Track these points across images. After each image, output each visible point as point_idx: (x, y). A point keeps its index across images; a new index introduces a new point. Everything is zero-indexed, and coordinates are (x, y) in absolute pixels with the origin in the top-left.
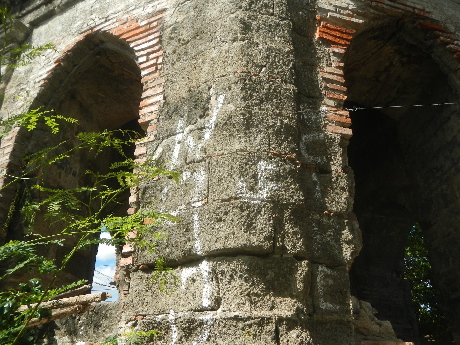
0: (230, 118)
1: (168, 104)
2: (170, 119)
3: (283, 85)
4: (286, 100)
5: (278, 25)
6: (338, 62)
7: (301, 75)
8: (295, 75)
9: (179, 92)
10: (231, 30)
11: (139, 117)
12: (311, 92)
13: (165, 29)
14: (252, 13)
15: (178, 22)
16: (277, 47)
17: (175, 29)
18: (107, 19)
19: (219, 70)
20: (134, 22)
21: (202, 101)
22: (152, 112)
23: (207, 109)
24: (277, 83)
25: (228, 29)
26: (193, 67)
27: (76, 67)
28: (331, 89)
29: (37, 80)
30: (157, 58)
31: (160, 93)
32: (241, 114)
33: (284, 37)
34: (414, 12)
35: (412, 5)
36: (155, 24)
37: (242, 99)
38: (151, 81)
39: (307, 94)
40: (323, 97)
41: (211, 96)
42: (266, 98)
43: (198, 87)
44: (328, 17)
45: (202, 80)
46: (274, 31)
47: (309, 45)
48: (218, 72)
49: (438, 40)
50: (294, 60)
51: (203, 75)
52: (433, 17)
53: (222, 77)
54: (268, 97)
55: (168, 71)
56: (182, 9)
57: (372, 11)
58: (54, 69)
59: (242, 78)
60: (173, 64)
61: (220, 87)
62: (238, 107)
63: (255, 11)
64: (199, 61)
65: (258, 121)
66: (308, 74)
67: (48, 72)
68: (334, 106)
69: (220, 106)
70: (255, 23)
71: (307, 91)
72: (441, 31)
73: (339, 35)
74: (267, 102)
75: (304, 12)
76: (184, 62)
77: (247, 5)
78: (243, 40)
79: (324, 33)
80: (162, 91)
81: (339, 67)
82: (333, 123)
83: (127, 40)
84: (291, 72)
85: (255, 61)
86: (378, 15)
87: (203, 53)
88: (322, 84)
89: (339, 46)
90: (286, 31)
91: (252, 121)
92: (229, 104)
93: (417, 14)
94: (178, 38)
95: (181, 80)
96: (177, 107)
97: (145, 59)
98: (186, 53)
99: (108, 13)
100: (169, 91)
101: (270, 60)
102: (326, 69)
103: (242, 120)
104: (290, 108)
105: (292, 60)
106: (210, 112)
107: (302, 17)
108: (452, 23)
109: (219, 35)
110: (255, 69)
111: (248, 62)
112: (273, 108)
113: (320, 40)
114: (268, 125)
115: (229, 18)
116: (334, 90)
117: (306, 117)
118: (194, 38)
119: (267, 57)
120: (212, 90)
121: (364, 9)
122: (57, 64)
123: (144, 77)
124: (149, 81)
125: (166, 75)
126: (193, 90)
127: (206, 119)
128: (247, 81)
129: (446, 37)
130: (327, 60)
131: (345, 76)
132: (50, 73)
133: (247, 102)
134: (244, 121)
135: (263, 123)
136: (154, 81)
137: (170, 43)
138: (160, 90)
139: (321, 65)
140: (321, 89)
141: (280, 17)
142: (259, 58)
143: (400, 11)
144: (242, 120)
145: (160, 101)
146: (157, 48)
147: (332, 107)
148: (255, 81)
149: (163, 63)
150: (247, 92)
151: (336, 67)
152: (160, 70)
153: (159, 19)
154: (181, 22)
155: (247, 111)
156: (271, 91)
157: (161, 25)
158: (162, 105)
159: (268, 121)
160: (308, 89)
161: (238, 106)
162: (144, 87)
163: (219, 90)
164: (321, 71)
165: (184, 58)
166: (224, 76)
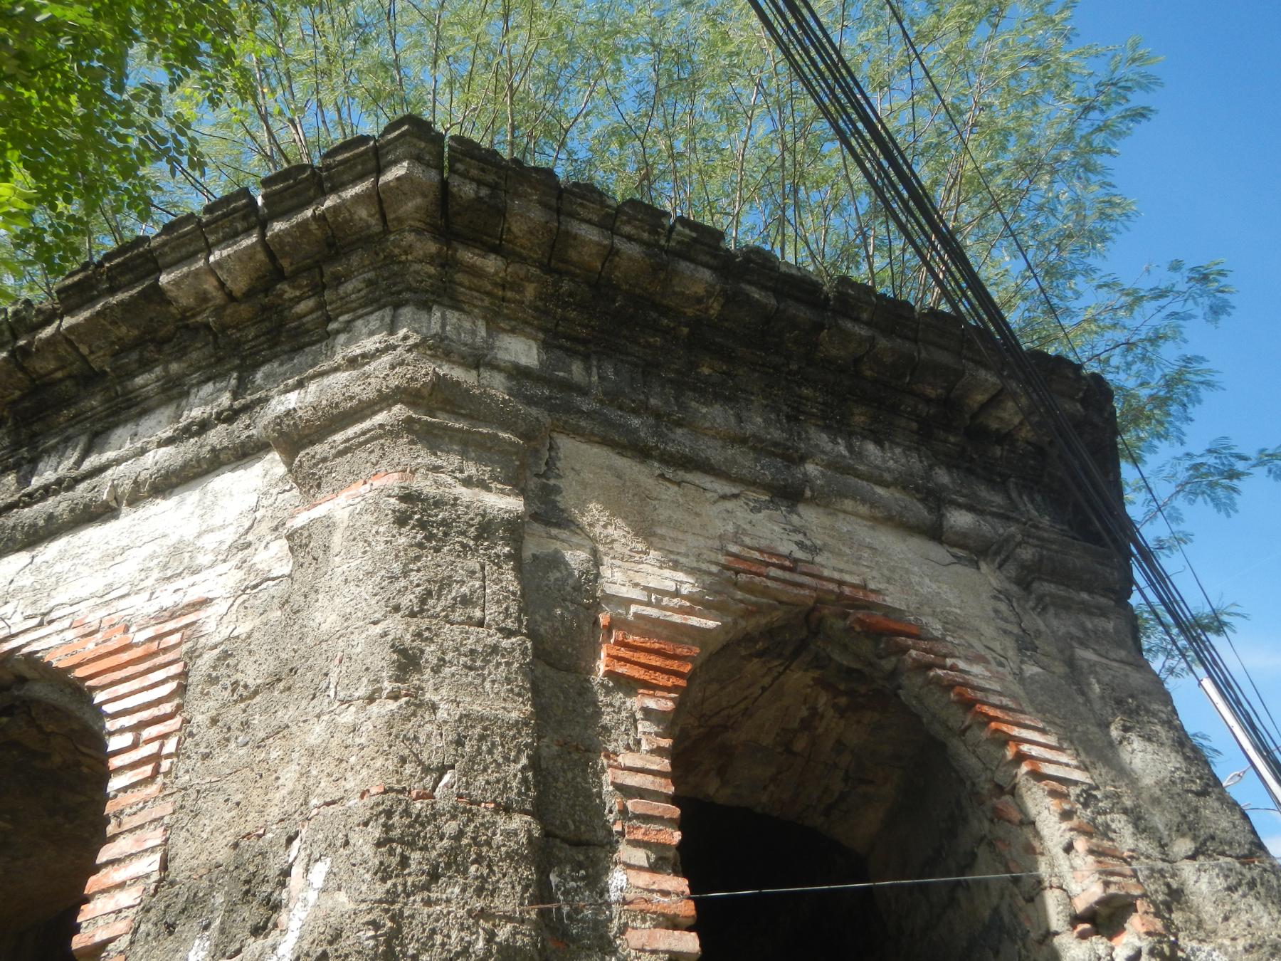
0: (337, 936)
1: (172, 884)
2: (171, 933)
3: (500, 820)
4: (505, 865)
5: (495, 649)
6: (657, 734)
7: (556, 780)
8: (535, 787)
9: (208, 844)
10: (367, 669)
11: (76, 929)
12: (583, 828)
13: (200, 655)
14: (425, 623)
15: (237, 637)
16: (486, 712)
17: (226, 655)
18: (47, 619)
19: (323, 784)
20: (118, 630)
21: (265, 880)
22: (120, 911)
23: (276, 907)
24: (483, 817)
25: (358, 667)
26: (256, 770)
28: (637, 817)
30: (165, 737)
31: (152, 850)
32: (368, 923)
33: (508, 681)
34: (842, 593)
35: (836, 575)
36: (174, 639)
37: (375, 874)
38: (135, 808)
39: (569, 839)
40: (617, 842)
41: (291, 866)
42: (448, 866)
43: (260, 836)
44: (630, 617)
45: (274, 812)
46: (483, 668)
47: (580, 694)
48: (319, 791)
49: (906, 657)
50: (532, 743)
51: (278, 796)
52: (889, 601)
53: (328, 804)
54: (454, 861)
55: (187, 777)
56: (251, 601)
57: (739, 595)
59: (381, 808)
60: (206, 756)
61: (320, 836)
62: (363, 901)
63: (436, 616)
64: (274, 755)
65: (418, 941)
66: (574, 778)
68: (646, 865)
69: (312, 896)
70: (433, 647)
71: (572, 827)
72: (909, 635)
73: (658, 664)
74: (450, 878)
75: (567, 608)
76: (237, 752)
77: (415, 601)
78: (395, 696)
79: (620, 659)
80: (159, 842)
81: (658, 751)
82: (644, 920)
83: (89, 683)
84: (524, 781)
85: (424, 757)
86: (755, 604)
87: (286, 732)
88: (613, 802)
89: (658, 693)
90: (516, 665)
91: (401, 945)
92: (339, 889)
93: (848, 598)
94: (233, 679)
95: (222, 806)
96: (195, 894)
97: (127, 739)
98: (245, 725)
99: (52, 603)
100: (180, 842)
101: (467, 749)
102: (626, 759)
103: (372, 943)
104: (518, 888)
105: (526, 745)
106: (283, 917)
107: (563, 622)
108: (934, 614)
109: (333, 681)
110: (422, 779)
111: (403, 760)
112: (467, 895)
113: (610, 679)
114: (449, 951)
115: (364, 635)
116: (646, 818)
117: (566, 909)
118: (270, 686)
119: (459, 742)
120: (296, 843)
121: (716, 592)
123: (115, 796)
124: (128, 811)
125: (179, 790)
126: (243, 843)
127: (270, 941)
128: (396, 818)
129: (925, 650)
130: (627, 732)
131: (676, 775)
133: (389, 883)
134: (376, 946)
135: (433, 945)
136: (142, 808)
137: (208, 694)
138: (154, 837)
139: (611, 748)
140: (611, 817)
141: (501, 630)
142: (435, 747)
143: (807, 592)
144: (372, 943)
145: (148, 876)
146: (167, 708)
147: (640, 868)
148: (418, 815)
149: (176, 754)
150: (391, 852)
151: (652, 752)
152: (166, 774)
153: (187, 626)
154: (243, 637)
155: (387, 911)
156: (464, 841)
157: (190, 644)
158: (153, 887)
159: (449, 937)
160: (574, 822)
161: (363, 896)
162: (111, 829)
163: (315, 846)
164: (610, 766)
165: (240, 739)
166: (334, 802)
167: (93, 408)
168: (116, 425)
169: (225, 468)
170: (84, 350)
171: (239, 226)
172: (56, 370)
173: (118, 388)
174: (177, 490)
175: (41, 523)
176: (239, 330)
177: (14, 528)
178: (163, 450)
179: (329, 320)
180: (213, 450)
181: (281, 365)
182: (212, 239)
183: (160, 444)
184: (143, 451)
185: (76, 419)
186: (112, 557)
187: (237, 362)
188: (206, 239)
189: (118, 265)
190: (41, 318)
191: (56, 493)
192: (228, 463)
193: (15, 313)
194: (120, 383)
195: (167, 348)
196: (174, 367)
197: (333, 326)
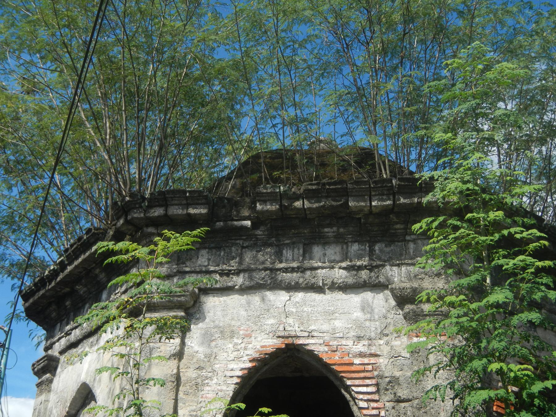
17: (390, 382)
27: (267, 367)
29: (229, 374)
36: (370, 368)
58: (249, 369)
67: (242, 369)
122: (254, 364)
132: (246, 372)
167: (304, 233)
168: (314, 244)
170: (308, 212)
171: (385, 193)
173: (317, 230)
174: (348, 291)
177: (281, 281)
178: (341, 271)
179: (407, 234)
180: (365, 281)
181: (386, 246)
182: (373, 193)
183: (340, 268)
184: (333, 268)
186: (330, 315)
187: (369, 239)
188: (370, 193)
189: (333, 189)
191: (297, 272)
192: (369, 287)
193: (284, 191)
196: (341, 230)
197: (408, 238)
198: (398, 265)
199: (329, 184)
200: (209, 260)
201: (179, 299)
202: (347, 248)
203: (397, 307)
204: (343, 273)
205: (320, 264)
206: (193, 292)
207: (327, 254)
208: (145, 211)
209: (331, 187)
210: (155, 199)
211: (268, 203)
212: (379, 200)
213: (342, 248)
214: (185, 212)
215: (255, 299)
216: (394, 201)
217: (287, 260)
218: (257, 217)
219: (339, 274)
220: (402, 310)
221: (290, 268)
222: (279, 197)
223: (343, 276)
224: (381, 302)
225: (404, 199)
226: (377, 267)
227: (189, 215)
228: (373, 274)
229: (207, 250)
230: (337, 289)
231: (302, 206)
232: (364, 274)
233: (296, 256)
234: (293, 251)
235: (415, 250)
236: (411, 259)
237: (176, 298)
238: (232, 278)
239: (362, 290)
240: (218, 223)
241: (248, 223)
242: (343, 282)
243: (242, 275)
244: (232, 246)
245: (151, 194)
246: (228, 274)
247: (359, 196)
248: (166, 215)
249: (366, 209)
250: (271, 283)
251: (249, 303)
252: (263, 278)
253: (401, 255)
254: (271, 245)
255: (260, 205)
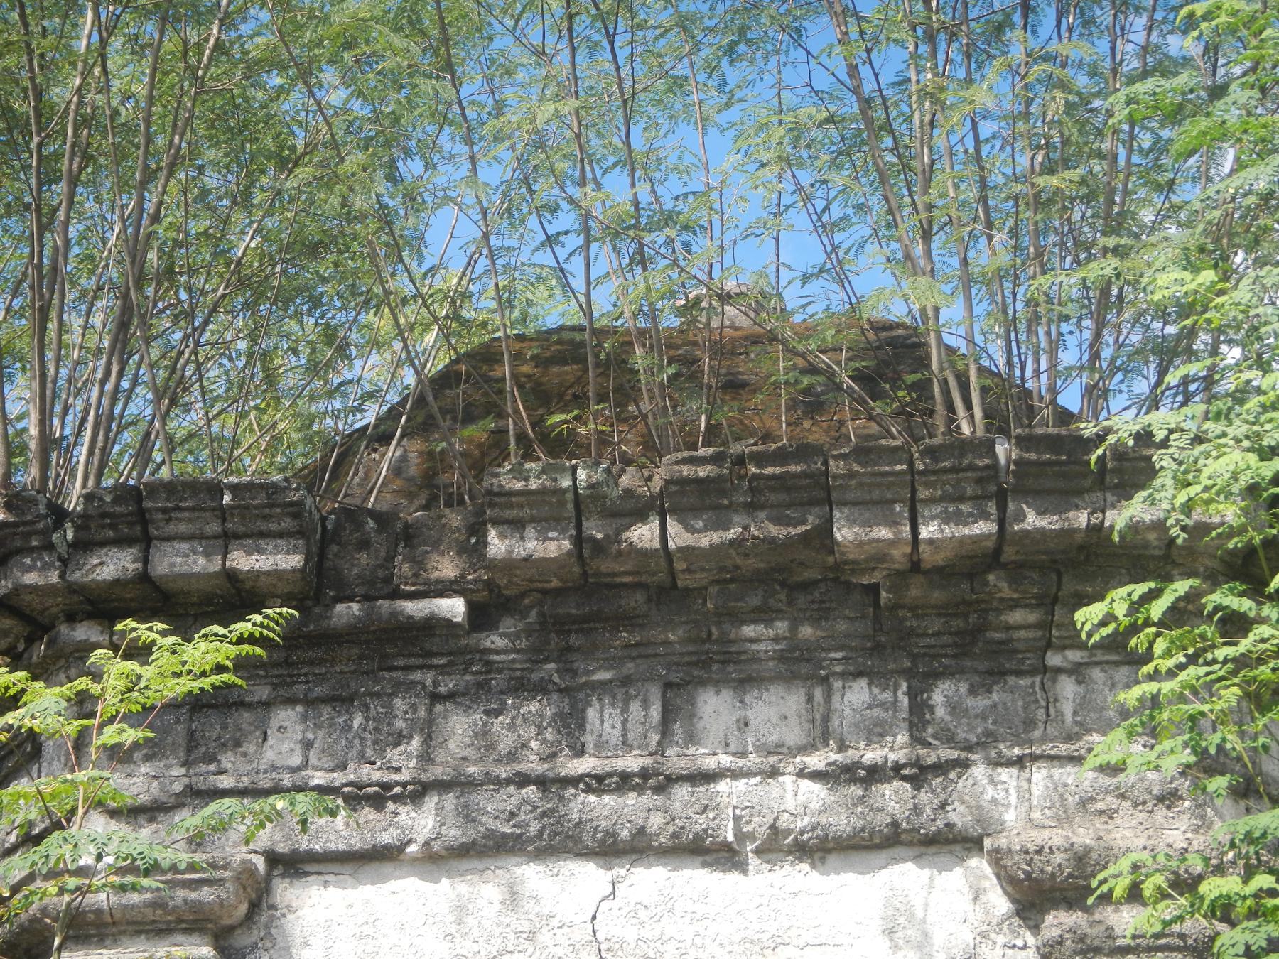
167: (666, 643)
168: (703, 683)
169: (898, 851)
170: (679, 565)
171: (969, 491)
172: (626, 573)
173: (714, 630)
174: (832, 859)
175: (624, 834)
176: (916, 616)
178: (806, 784)
179: (1049, 645)
180: (895, 824)
181: (973, 691)
182: (923, 493)
183: (801, 774)
184: (774, 773)
185: (638, 651)
187: (907, 664)
188: (914, 491)
190: (631, 504)
191: (640, 789)
192: (910, 844)
193: (591, 486)
194: (719, 624)
195: (801, 600)
196: (806, 631)
197: (1054, 659)
198: (1020, 762)
199: (760, 459)
200: (307, 745)
201: (193, 895)
202: (828, 698)
203: (1016, 921)
204: (815, 792)
205: (726, 760)
206: (248, 870)
207: (753, 722)
208: (64, 562)
209: (769, 470)
210: (104, 515)
211: (530, 532)
212: (947, 519)
213: (810, 699)
214: (216, 566)
215: (482, 891)
216: (1002, 523)
217: (600, 746)
218: (489, 585)
219: (800, 799)
220: (1036, 929)
221: (611, 775)
222: (570, 506)
223: (815, 805)
224: (956, 901)
225: (1041, 513)
226: (940, 768)
227: (231, 576)
228: (924, 796)
229: (299, 708)
230: (789, 853)
231: (656, 544)
232: (893, 798)
233: (635, 729)
234: (625, 710)
235: (1083, 704)
236: (1069, 738)
237: (181, 893)
238: (396, 813)
239: (883, 856)
240: (340, 607)
241: (454, 607)
242: (814, 829)
243: (431, 801)
244: (392, 695)
245: (89, 498)
246: (379, 797)
247: (873, 505)
248: (144, 577)
249: (896, 553)
250: (541, 832)
251: (461, 911)
252: (513, 815)
253: (1030, 724)
254: (541, 689)
255: (502, 536)
